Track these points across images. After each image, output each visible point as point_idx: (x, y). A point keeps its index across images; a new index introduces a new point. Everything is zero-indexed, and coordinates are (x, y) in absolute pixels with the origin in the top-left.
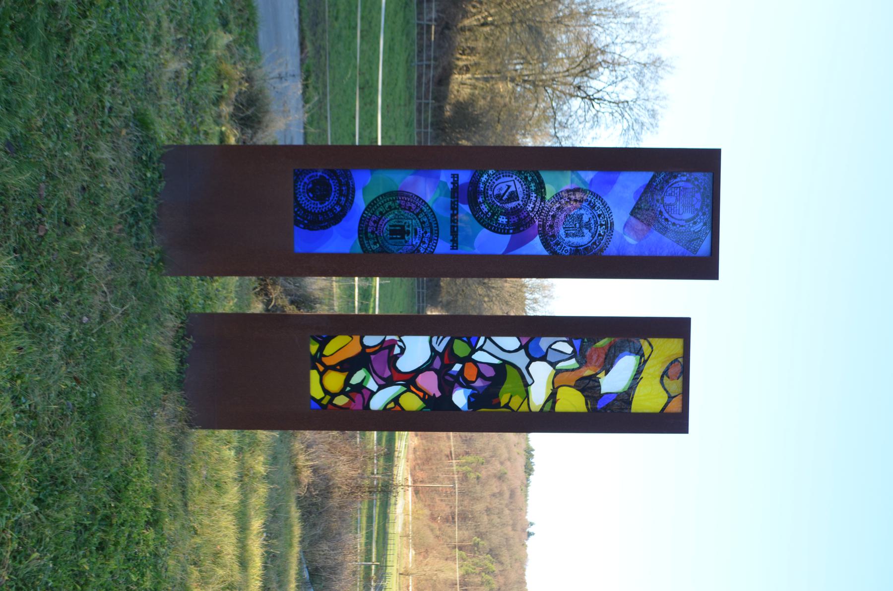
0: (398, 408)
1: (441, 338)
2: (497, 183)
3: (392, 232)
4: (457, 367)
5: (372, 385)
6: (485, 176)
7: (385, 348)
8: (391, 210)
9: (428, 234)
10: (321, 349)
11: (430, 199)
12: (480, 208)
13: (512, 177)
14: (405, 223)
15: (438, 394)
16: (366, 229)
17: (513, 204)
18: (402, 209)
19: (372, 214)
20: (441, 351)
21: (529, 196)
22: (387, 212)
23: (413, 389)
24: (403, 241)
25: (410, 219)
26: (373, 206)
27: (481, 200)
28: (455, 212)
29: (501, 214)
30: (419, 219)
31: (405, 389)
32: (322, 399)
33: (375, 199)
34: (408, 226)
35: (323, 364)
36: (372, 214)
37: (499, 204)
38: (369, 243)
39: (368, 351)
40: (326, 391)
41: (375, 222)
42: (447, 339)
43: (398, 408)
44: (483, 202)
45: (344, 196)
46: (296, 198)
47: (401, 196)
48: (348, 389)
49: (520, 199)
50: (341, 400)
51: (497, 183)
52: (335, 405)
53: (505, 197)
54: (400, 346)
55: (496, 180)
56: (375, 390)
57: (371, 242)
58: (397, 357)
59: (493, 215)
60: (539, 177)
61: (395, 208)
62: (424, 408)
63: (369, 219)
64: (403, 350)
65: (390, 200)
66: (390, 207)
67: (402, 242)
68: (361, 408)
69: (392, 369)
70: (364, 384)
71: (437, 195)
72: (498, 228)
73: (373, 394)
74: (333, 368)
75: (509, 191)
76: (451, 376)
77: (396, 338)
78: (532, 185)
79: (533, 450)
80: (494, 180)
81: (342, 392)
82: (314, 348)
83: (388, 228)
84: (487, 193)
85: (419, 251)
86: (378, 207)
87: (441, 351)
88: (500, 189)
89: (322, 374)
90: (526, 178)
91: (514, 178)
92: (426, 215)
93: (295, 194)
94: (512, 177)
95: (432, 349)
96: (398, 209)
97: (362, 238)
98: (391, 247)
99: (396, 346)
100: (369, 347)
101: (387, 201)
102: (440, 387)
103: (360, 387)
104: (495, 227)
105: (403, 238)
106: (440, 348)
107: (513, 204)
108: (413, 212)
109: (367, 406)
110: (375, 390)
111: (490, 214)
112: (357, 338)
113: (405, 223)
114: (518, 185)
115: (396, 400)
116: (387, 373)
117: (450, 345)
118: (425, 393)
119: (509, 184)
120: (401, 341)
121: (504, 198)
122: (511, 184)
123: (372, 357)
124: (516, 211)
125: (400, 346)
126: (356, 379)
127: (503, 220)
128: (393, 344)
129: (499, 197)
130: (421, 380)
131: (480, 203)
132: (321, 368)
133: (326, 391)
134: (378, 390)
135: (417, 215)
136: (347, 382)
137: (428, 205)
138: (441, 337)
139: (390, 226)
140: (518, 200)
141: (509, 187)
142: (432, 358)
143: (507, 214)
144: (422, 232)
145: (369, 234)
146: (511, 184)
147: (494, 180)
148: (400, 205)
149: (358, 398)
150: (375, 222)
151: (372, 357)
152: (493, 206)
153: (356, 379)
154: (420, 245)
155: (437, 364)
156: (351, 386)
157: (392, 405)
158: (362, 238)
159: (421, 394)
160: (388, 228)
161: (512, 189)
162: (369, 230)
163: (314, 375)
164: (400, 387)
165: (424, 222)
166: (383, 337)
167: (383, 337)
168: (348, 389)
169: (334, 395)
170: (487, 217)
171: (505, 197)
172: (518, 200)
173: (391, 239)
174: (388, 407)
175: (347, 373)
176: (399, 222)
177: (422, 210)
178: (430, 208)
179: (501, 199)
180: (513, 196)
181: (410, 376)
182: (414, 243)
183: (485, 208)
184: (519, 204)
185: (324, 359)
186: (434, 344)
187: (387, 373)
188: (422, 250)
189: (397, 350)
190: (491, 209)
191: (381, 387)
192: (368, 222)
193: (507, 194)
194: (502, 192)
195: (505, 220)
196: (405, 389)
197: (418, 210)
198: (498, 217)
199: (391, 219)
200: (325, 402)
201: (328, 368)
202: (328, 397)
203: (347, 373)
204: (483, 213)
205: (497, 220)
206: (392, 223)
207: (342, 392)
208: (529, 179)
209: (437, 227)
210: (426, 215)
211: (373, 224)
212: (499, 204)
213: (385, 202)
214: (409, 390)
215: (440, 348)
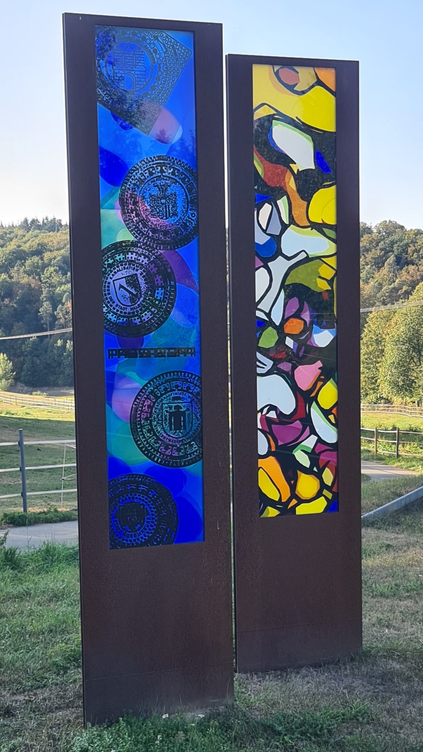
0: (334, 411)
1: (258, 363)
2: (117, 302)
3: (178, 427)
4: (289, 342)
5: (310, 442)
6: (110, 316)
7: (270, 428)
8: (153, 430)
9: (178, 383)
10: (273, 504)
11: (138, 383)
12: (147, 322)
13: (109, 283)
14: (167, 411)
15: (319, 364)
16: (175, 458)
17: (141, 281)
18: (151, 416)
19: (158, 452)
20: (272, 362)
21: (131, 262)
22: (155, 434)
23: (313, 395)
24: (187, 413)
25: (162, 407)
26: (149, 451)
27: (138, 321)
28: (152, 351)
29: (153, 296)
30: (162, 395)
31: (314, 403)
32: (326, 498)
33: (141, 449)
34: (170, 408)
35: (290, 500)
36: (158, 452)
37: (142, 299)
38: (190, 454)
39: (273, 449)
40: (319, 494)
41: (166, 448)
42: (259, 356)
43: (334, 411)
44: (140, 318)
45: (138, 487)
46: (142, 545)
47: (136, 418)
48: (315, 469)
49: (135, 272)
50: (328, 477)
51: (117, 302)
52: (333, 483)
53: (133, 291)
54: (268, 412)
55: (114, 302)
56: (316, 438)
57: (189, 451)
58: (280, 414)
59: (155, 306)
60: (108, 249)
61: (151, 424)
62: (334, 380)
63: (164, 455)
64: (272, 408)
65: (142, 431)
66: (149, 431)
67: (189, 414)
68: (335, 453)
69: (293, 419)
70: (310, 451)
71: (133, 375)
72: (170, 299)
73: (320, 440)
74: (293, 488)
75: (126, 286)
76: (299, 349)
77: (259, 415)
78: (118, 258)
79: (26, 220)
80: (114, 305)
81: (319, 475)
82: (272, 512)
83: (173, 431)
84: (129, 313)
85: (198, 393)
86: (150, 446)
87: (272, 362)
88: (124, 297)
89: (301, 501)
90: (110, 266)
91: (111, 281)
92: (157, 387)
93: (138, 545)
94: (109, 283)
95: (268, 373)
96: (151, 421)
97: (185, 462)
98: (194, 428)
99: (267, 415)
100: (270, 447)
101: (143, 434)
102: (312, 362)
103: (313, 455)
104: (169, 303)
105: (183, 413)
106: (269, 363)
107: (141, 281)
108: (154, 403)
109: (334, 447)
110: (316, 438)
111: (153, 310)
112: (261, 462)
113: (167, 411)
114: (119, 275)
115: (326, 413)
116: (298, 424)
117: (265, 352)
118: (318, 379)
119: (117, 287)
120: (262, 410)
121: (135, 293)
122: (117, 283)
123: (280, 443)
124: (149, 278)
125: (268, 412)
126: (304, 460)
127: (159, 293)
128: (268, 421)
129: (133, 298)
130: (304, 385)
131: (141, 321)
132: (294, 502)
133: (319, 494)
134: (316, 434)
135: (157, 398)
136: (307, 471)
137: (146, 385)
138: (258, 363)
139: (171, 429)
140: (136, 275)
141: (121, 286)
142: (280, 373)
143: (152, 289)
144: (176, 391)
145: (181, 454)
146: (117, 283)
147: (114, 305)
148: (146, 419)
149: (323, 458)
150: (166, 448)
151: (280, 443)
152: (144, 306)
153: (304, 460)
154: (191, 393)
155: (286, 366)
156: (312, 466)
157: (331, 417)
158: (185, 462)
159: (320, 384)
160: (173, 431)
161: (123, 282)
162: (176, 454)
163: (302, 510)
164: (312, 409)
165: (165, 389)
166: (259, 432)
167: (259, 432)
168: (315, 469)
169: (323, 486)
170: (157, 313)
171: (133, 291)
172: (136, 275)
173: (185, 428)
174: (333, 422)
175: (299, 472)
176: (166, 419)
177: (152, 392)
178: (149, 383)
179: (136, 295)
180: (132, 281)
181: (301, 399)
182: (189, 400)
183: (146, 316)
184: (141, 274)
185: (284, 500)
186: (264, 371)
187: (298, 424)
188: (197, 390)
189: (272, 415)
190: (148, 308)
191: (313, 432)
192: (167, 456)
193: (129, 288)
194: (128, 295)
195: (160, 291)
196: (314, 403)
197: (152, 397)
198: (156, 300)
199: (163, 428)
200: (330, 496)
201: (294, 495)
202: (325, 492)
203: (299, 472)
204: (152, 318)
205: (160, 301)
206: (167, 427)
207: (319, 475)
208: (111, 261)
209: (170, 373)
210: (157, 387)
211: (169, 450)
212: (142, 299)
213: (144, 437)
214: (315, 399)
215: (269, 363)
